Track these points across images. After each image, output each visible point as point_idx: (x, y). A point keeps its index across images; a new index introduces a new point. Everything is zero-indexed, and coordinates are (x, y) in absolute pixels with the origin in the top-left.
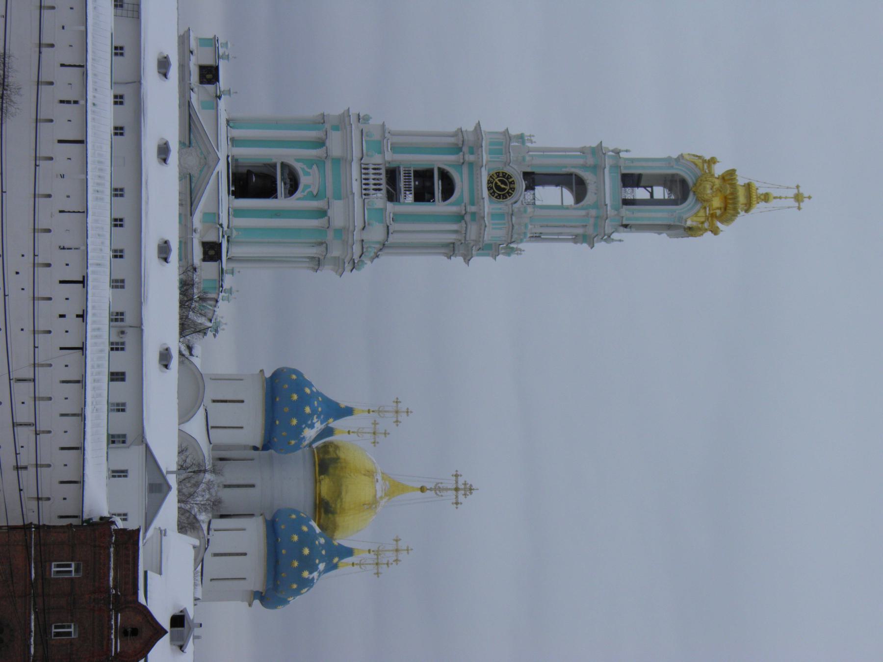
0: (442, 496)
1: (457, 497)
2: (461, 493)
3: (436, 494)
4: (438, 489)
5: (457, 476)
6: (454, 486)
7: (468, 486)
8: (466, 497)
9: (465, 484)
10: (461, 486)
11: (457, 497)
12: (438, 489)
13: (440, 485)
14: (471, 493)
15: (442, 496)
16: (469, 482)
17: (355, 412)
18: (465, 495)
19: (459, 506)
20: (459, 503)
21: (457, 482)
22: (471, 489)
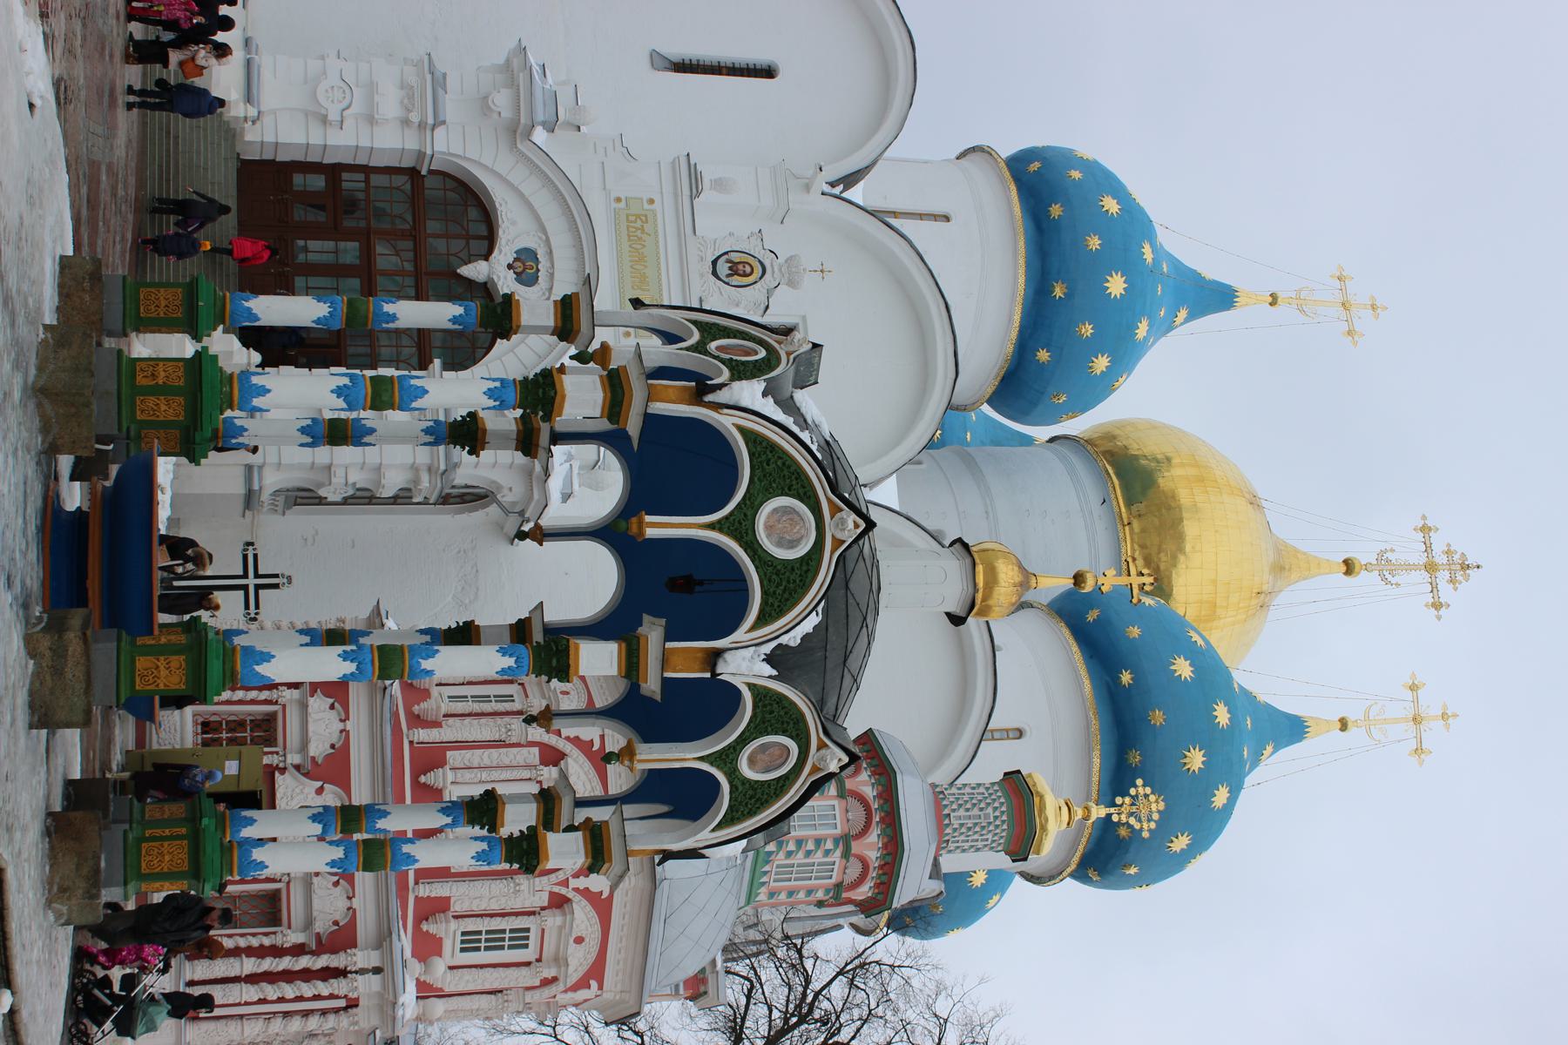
0: (1398, 585)
1: (1434, 588)
2: (1443, 576)
3: (1384, 579)
4: (1386, 567)
5: (1425, 529)
6: (1423, 559)
7: (1456, 557)
8: (1456, 589)
9: (1448, 552)
10: (1441, 559)
11: (1434, 588)
12: (1386, 567)
13: (1389, 555)
14: (1467, 578)
15: (1398, 585)
16: (1458, 548)
17: (1240, 300)
18: (1452, 581)
19: (1443, 611)
20: (1441, 605)
21: (1428, 549)
22: (1465, 567)
